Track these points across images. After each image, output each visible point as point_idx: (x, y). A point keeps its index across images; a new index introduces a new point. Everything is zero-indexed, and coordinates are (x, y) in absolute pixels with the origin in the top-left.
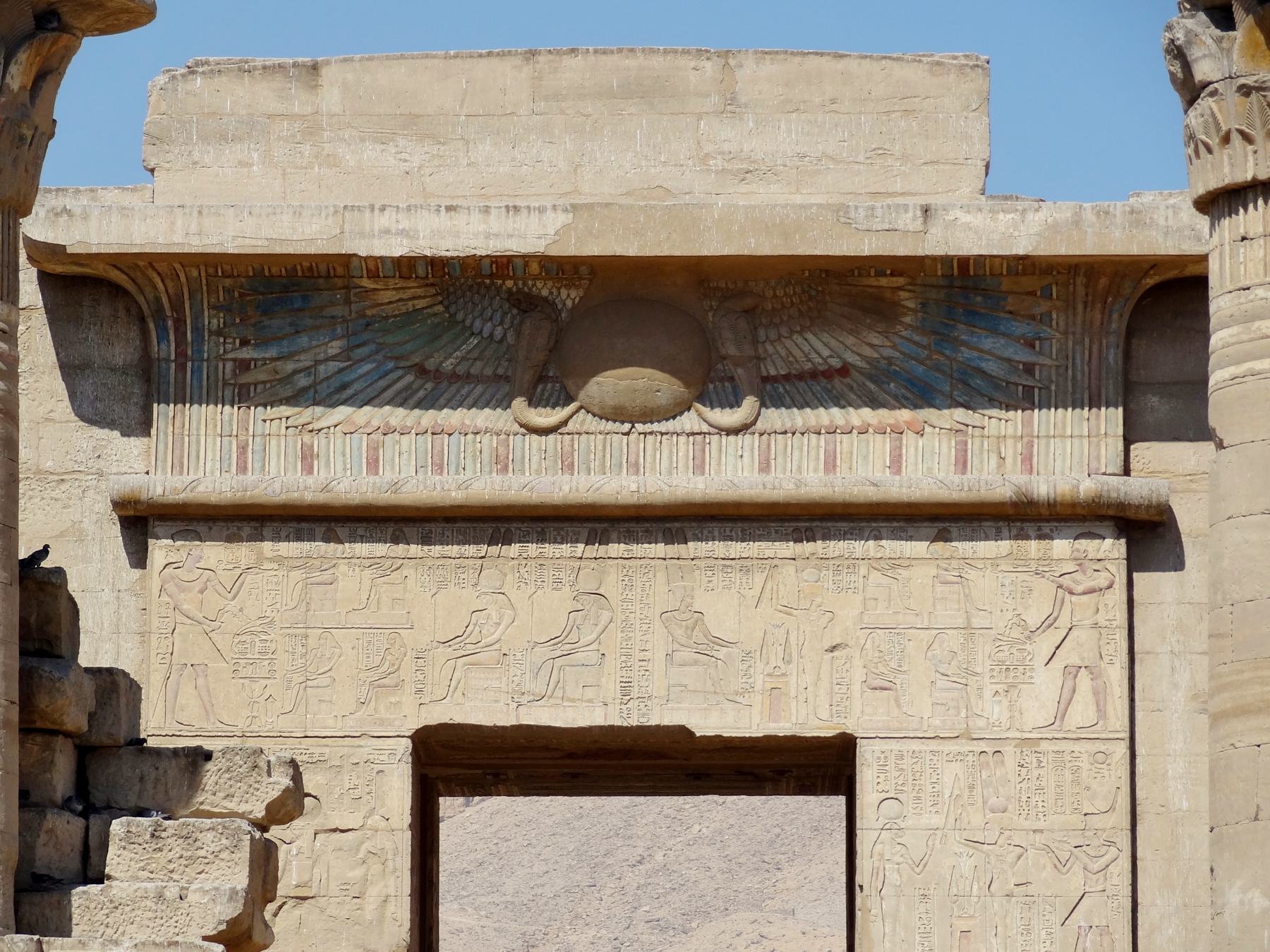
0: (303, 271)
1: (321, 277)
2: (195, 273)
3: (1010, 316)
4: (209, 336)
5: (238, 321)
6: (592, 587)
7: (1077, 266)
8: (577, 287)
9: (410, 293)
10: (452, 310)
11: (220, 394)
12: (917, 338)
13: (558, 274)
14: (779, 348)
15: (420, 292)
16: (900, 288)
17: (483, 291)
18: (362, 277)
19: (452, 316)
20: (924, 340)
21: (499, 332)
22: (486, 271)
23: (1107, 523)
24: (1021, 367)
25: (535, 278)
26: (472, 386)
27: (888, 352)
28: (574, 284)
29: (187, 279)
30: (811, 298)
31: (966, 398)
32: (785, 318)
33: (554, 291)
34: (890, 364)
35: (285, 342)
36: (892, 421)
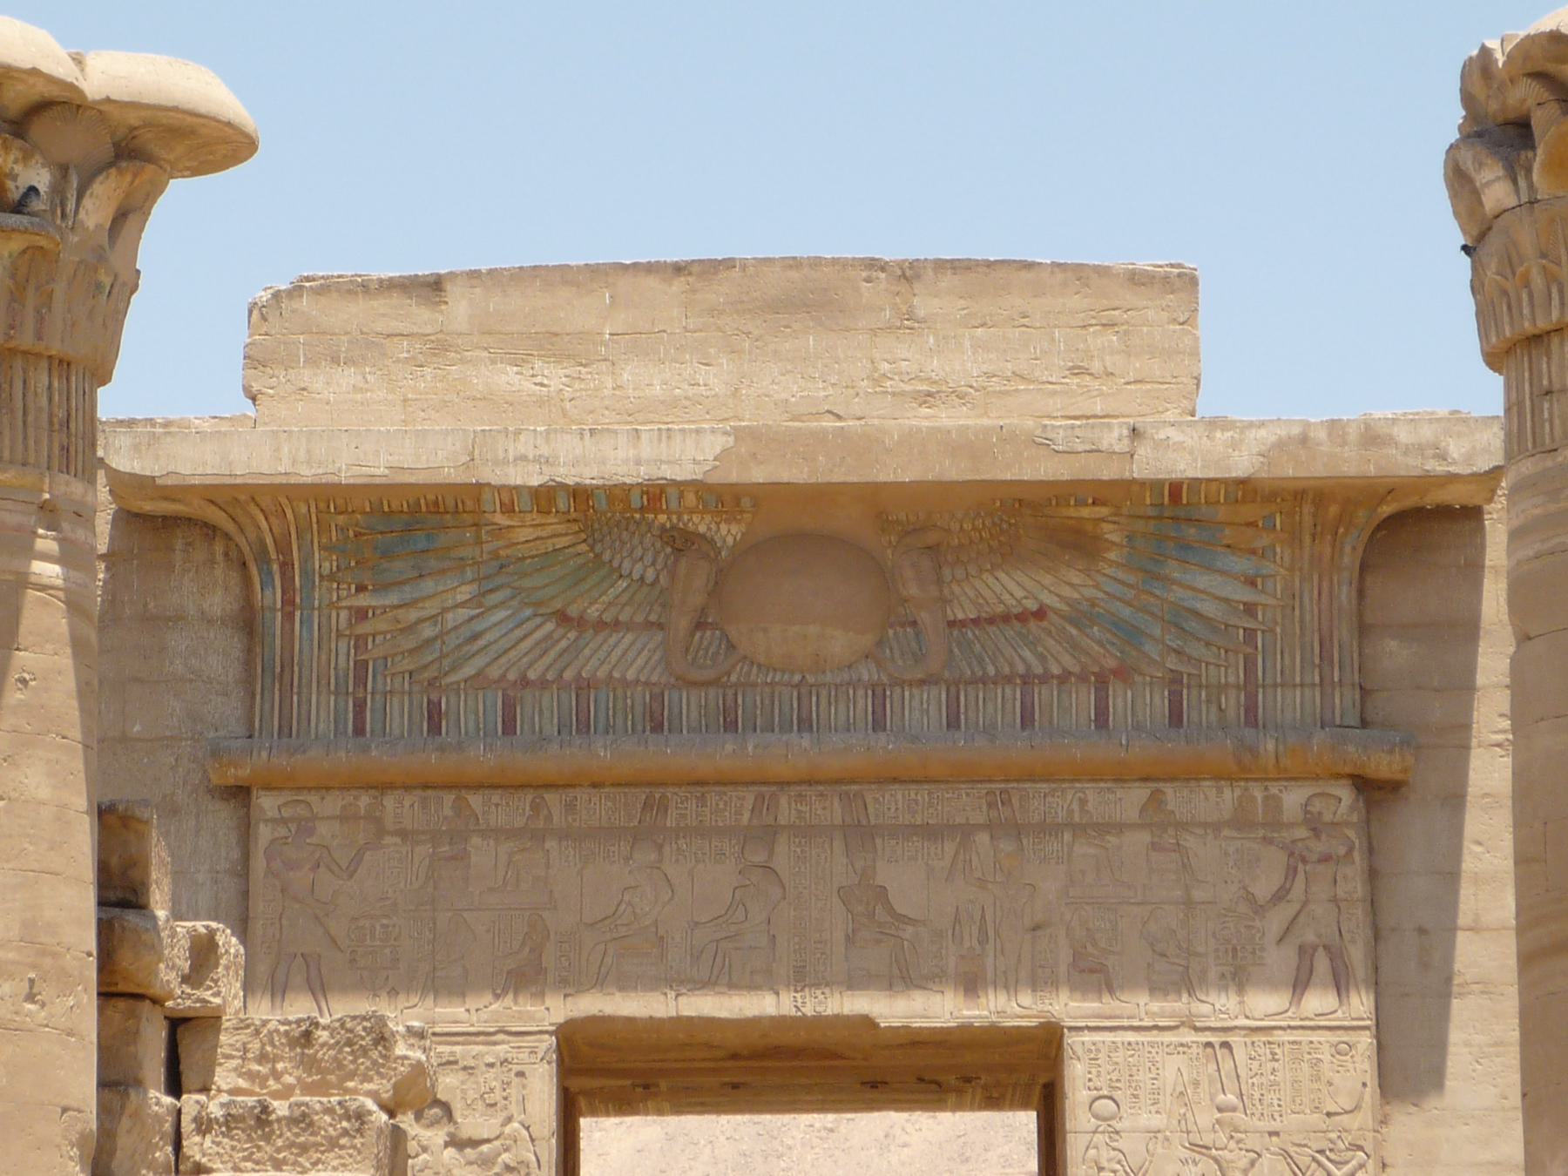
0: (427, 505)
1: (448, 512)
2: (304, 509)
3: (1229, 550)
4: (320, 581)
5: (353, 564)
6: (759, 858)
7: (1304, 492)
8: (739, 522)
10: (598, 548)
11: (333, 646)
12: (1121, 575)
13: (716, 507)
14: (967, 590)
15: (561, 528)
16: (1103, 520)
17: (632, 527)
18: (495, 512)
19: (597, 556)
20: (1131, 579)
21: (650, 575)
22: (636, 503)
23: (1343, 782)
24: (1241, 607)
25: (692, 512)
26: (622, 634)
27: (1090, 592)
28: (735, 518)
29: (294, 516)
31: (1179, 642)
32: (973, 555)
33: (713, 526)
34: (1093, 605)
35: (407, 588)
36: (1096, 669)
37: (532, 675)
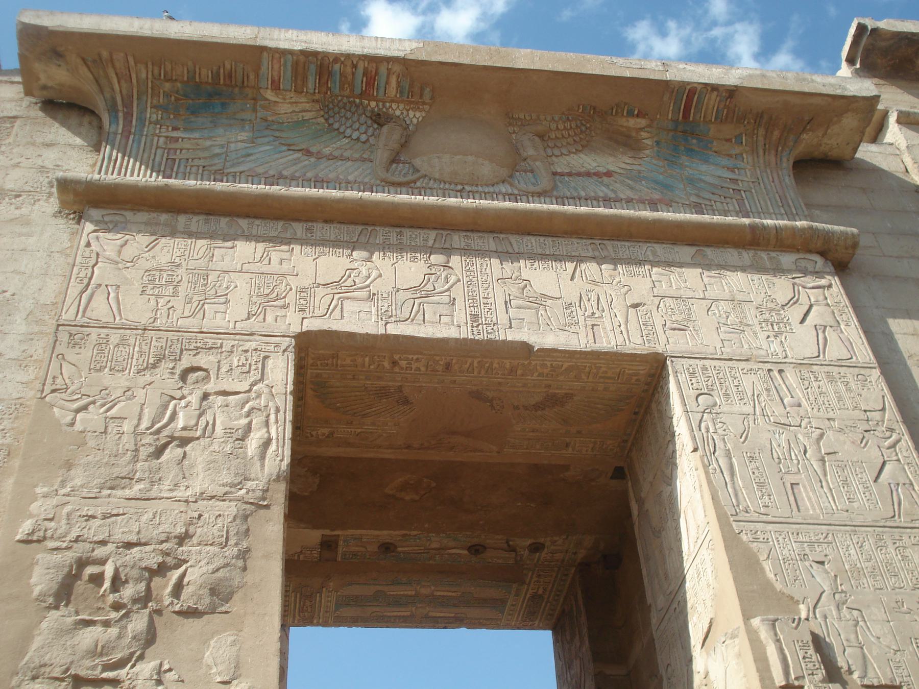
2: (144, 76)
5: (172, 116)
9: (300, 107)
10: (331, 121)
12: (655, 162)
13: (408, 97)
15: (308, 106)
16: (641, 129)
17: (353, 109)
18: (267, 88)
19: (330, 125)
20: (661, 164)
21: (364, 137)
22: (358, 91)
25: (392, 101)
27: (638, 168)
28: (418, 108)
30: (582, 132)
33: (405, 112)
35: (206, 131)
37: (285, 173)
